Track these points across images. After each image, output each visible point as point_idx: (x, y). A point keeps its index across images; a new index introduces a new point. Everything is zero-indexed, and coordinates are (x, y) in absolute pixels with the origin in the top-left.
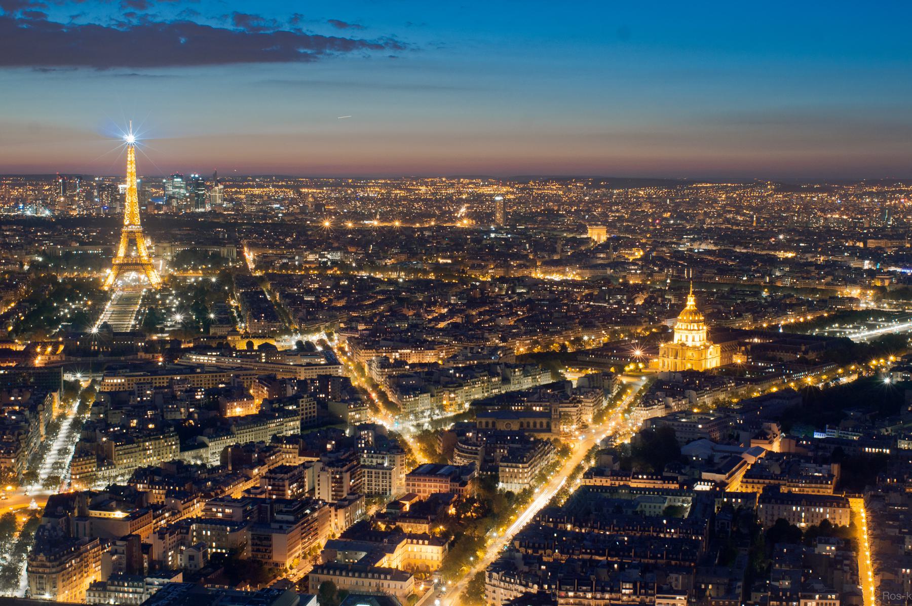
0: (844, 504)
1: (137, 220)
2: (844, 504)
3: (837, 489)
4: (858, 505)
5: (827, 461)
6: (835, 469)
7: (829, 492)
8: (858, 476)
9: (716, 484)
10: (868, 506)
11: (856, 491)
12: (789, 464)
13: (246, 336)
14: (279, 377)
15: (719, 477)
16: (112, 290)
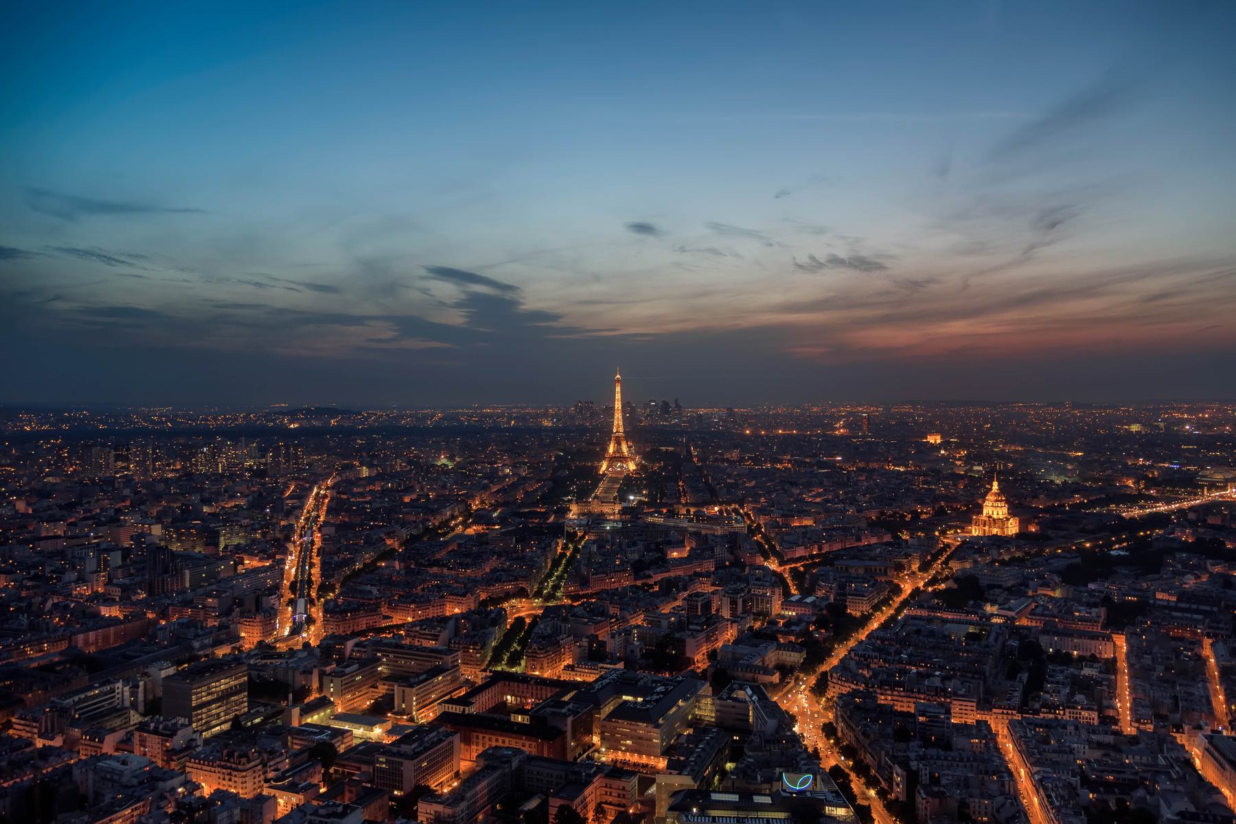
0: (1109, 638)
1: (621, 430)
2: (1109, 638)
3: (1104, 627)
4: (1121, 642)
5: (1095, 605)
6: (1102, 611)
7: (1098, 629)
8: (1120, 617)
9: (1008, 618)
10: (1127, 641)
11: (1119, 629)
12: (1064, 608)
13: (687, 504)
14: (703, 532)
15: (1010, 614)
16: (604, 474)
